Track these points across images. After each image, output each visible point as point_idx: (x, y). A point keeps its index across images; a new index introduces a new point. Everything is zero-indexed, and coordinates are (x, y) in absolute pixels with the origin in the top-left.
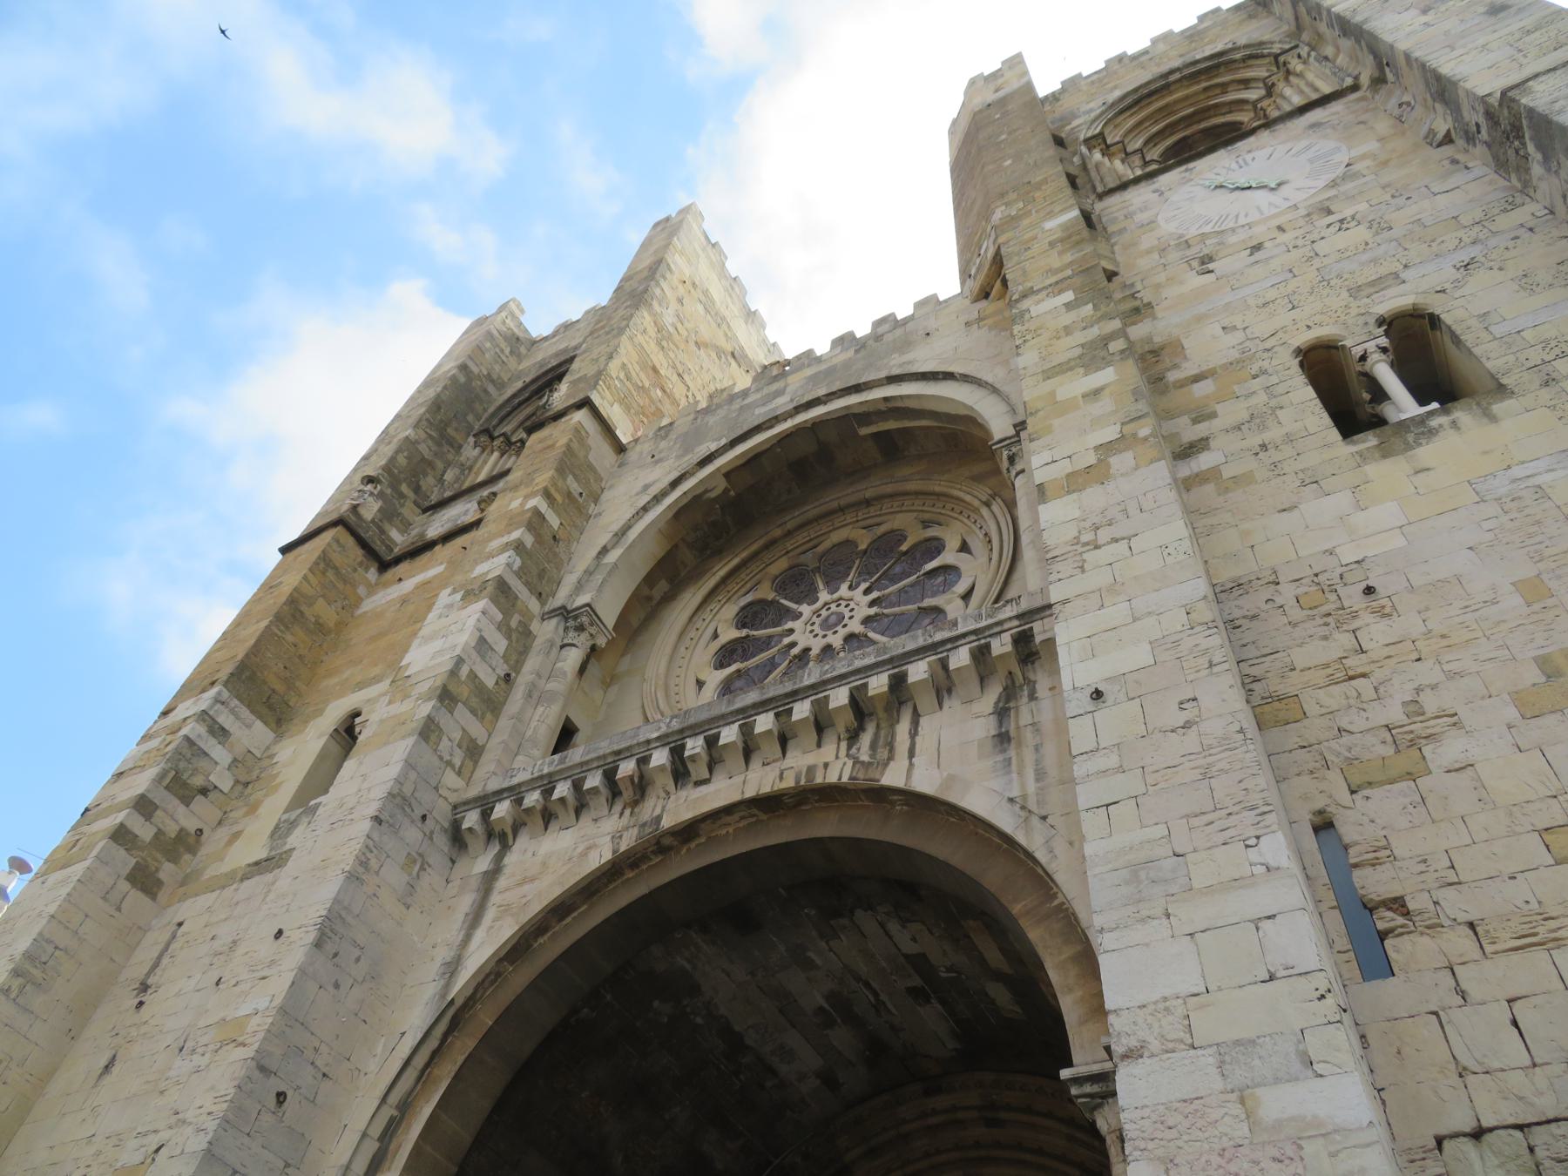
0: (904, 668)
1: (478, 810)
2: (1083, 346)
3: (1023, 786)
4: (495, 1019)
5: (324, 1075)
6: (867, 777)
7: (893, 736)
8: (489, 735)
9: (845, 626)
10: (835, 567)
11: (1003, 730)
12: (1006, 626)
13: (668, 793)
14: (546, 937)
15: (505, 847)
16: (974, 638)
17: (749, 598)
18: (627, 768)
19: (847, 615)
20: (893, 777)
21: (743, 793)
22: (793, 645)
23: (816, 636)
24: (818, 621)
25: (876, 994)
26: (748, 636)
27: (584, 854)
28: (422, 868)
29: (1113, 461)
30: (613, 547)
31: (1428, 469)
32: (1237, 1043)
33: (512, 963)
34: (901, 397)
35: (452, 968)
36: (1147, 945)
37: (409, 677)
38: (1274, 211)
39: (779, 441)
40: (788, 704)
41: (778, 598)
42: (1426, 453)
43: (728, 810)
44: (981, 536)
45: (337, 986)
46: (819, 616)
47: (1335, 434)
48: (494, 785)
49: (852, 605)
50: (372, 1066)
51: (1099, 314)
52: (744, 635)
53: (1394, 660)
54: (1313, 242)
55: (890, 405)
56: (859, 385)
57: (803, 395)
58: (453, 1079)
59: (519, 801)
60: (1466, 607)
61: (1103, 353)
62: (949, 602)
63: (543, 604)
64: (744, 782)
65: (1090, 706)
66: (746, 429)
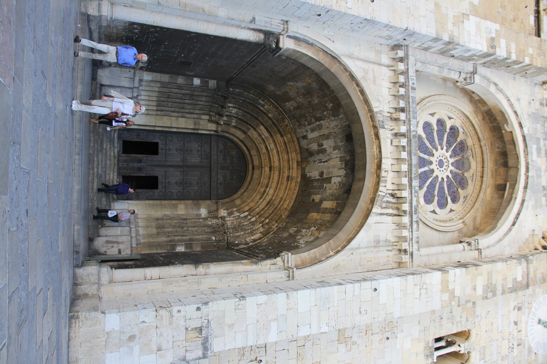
0: (408, 215)
1: (403, 56)
2: (495, 284)
3: (362, 248)
4: (334, 72)
5: (324, 23)
6: (378, 200)
8: (432, 52)
9: (438, 169)
10: (461, 164)
11: (380, 242)
12: (411, 247)
13: (391, 130)
14: (355, 86)
15: (388, 66)
16: (410, 238)
17: (461, 130)
18: (403, 116)
19: (441, 169)
20: (376, 209)
21: (384, 158)
22: (437, 150)
23: (438, 158)
24: (443, 159)
25: (324, 162)
26: (446, 132)
27: (378, 100)
28: (387, 39)
29: (447, 294)
30: (497, 88)
31: (417, 356)
32: (286, 319)
33: (349, 75)
34: (514, 204)
35: (350, 57)
36: (310, 301)
37: (463, 22)
39: (517, 154)
40: (408, 176)
41: (457, 142)
42: (422, 357)
43: (380, 152)
44: (453, 217)
45: (351, 24)
46: (445, 159)
47: (437, 336)
48: (411, 59)
49: (445, 171)
50: (326, 32)
51: (506, 289)
52: (447, 130)
53: (368, 341)
55: (513, 198)
56: (527, 189)
57: (533, 166)
58: (318, 61)
59: (402, 73)
60: (376, 358)
61: (489, 291)
62: (434, 206)
63: (480, 64)
64: (388, 158)
65: (373, 288)
66: (527, 142)
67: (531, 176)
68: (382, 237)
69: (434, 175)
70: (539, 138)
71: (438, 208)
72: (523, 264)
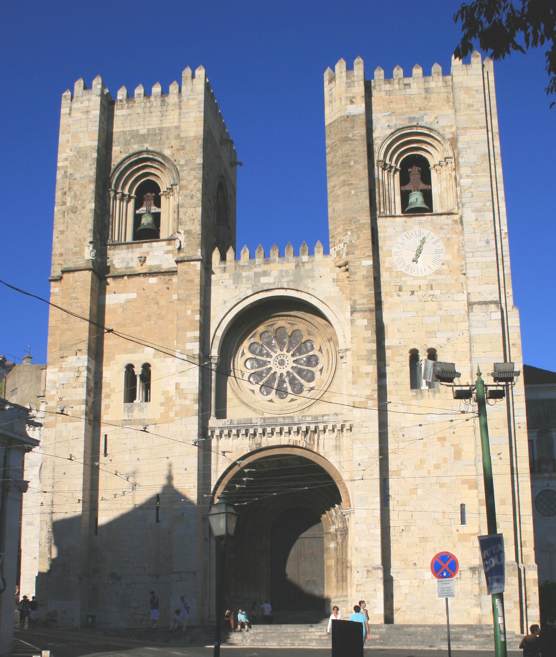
7: (314, 439)
9: (286, 367)
13: (261, 437)
17: (252, 340)
18: (251, 431)
22: (271, 368)
23: (277, 367)
24: (278, 360)
35: (217, 471)
37: (182, 389)
38: (421, 275)
42: (422, 402)
46: (277, 359)
49: (288, 359)
54: (425, 301)
66: (259, 290)
67: (288, 285)
68: (333, 443)
69: (291, 371)
70: (255, 273)
71: (317, 366)
72: (354, 318)
